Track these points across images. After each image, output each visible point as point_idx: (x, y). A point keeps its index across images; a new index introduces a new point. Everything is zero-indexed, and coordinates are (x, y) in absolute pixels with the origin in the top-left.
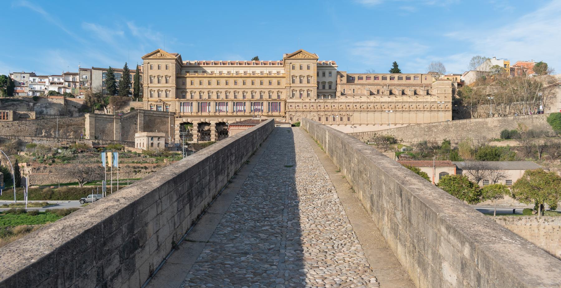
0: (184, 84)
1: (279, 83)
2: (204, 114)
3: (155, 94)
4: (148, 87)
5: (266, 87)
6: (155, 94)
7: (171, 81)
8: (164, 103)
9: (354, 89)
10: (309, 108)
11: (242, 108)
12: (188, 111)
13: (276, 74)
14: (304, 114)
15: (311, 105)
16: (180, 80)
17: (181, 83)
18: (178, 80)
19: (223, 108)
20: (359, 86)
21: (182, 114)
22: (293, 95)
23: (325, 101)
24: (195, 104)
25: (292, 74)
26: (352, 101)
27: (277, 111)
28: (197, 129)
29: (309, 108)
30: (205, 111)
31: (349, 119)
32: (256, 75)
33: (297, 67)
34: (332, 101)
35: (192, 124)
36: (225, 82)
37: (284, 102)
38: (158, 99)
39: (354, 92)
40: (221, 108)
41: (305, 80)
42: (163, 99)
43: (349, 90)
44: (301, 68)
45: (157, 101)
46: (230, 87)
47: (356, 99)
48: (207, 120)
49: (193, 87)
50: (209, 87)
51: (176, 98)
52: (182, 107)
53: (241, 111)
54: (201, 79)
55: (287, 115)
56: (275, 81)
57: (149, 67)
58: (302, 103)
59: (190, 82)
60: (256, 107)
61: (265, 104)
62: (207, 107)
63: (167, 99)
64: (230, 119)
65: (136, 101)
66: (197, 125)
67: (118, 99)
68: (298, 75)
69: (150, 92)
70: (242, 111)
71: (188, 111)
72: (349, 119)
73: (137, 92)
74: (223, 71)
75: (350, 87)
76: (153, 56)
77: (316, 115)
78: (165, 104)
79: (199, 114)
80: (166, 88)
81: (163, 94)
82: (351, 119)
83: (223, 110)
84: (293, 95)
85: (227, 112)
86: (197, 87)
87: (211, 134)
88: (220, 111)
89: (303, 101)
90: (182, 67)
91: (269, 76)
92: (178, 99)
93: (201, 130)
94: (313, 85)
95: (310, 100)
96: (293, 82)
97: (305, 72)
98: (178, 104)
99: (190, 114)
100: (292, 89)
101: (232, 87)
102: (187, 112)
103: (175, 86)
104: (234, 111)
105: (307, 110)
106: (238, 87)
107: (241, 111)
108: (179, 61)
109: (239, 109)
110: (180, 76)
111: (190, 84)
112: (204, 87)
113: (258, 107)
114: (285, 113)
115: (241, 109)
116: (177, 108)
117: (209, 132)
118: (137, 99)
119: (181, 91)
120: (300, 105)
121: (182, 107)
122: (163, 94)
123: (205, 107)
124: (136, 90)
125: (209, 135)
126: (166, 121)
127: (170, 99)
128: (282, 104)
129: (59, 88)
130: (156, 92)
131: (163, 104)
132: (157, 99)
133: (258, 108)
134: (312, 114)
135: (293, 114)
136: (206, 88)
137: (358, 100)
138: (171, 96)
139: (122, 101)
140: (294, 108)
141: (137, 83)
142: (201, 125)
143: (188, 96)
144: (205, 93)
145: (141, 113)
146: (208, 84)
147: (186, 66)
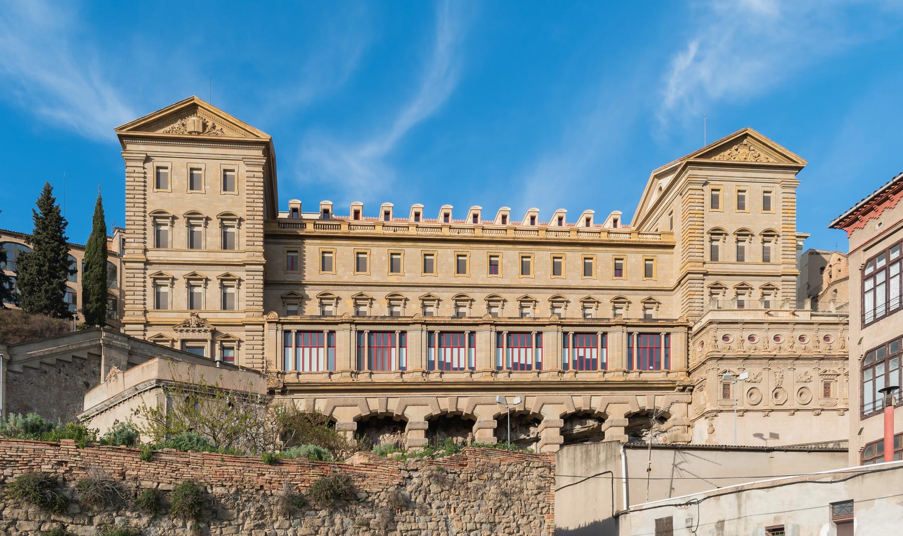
0: (295, 263)
2: (380, 377)
3: (178, 296)
4: (147, 263)
6: (178, 296)
7: (243, 240)
8: (214, 333)
10: (792, 347)
11: (527, 356)
12: (314, 369)
14: (774, 369)
15: (797, 334)
16: (280, 249)
17: (282, 260)
18: (273, 247)
19: (457, 356)
21: (290, 378)
24: (345, 338)
25: (709, 226)
27: (658, 367)
29: (792, 347)
30: (385, 367)
33: (728, 195)
36: (453, 260)
40: (448, 354)
41: (753, 248)
42: (212, 318)
48: (394, 405)
49: (328, 277)
50: (393, 279)
51: (264, 313)
52: (291, 351)
53: (526, 367)
54: (361, 245)
58: (766, 326)
59: (318, 258)
60: (581, 351)
61: (617, 339)
63: (225, 316)
64: (483, 401)
67: (10, 320)
69: (156, 286)
70: (529, 367)
71: (314, 369)
73: (95, 305)
77: (815, 375)
78: (218, 338)
79: (363, 378)
81: (211, 295)
83: (455, 365)
85: (472, 370)
86: (346, 279)
88: (445, 367)
89: (770, 319)
92: (274, 315)
94: (780, 269)
95: (794, 314)
96: (714, 257)
97: (758, 222)
98: (273, 335)
99: (323, 378)
100: (710, 281)
101: (480, 282)
102: (310, 373)
103: (263, 260)
104: (499, 369)
105: (784, 353)
107: (526, 367)
109: (516, 360)
111: (318, 264)
112: (375, 278)
113: (588, 350)
115: (523, 362)
116: (271, 353)
120: (759, 334)
121: (291, 351)
122: (211, 295)
123: (386, 353)
124: (92, 298)
128: (677, 339)
130: (181, 285)
131: (208, 336)
133: (588, 356)
134: (802, 368)
138: (243, 305)
139: (26, 327)
141: (97, 270)
143: (312, 308)
144: (375, 304)
146: (387, 267)
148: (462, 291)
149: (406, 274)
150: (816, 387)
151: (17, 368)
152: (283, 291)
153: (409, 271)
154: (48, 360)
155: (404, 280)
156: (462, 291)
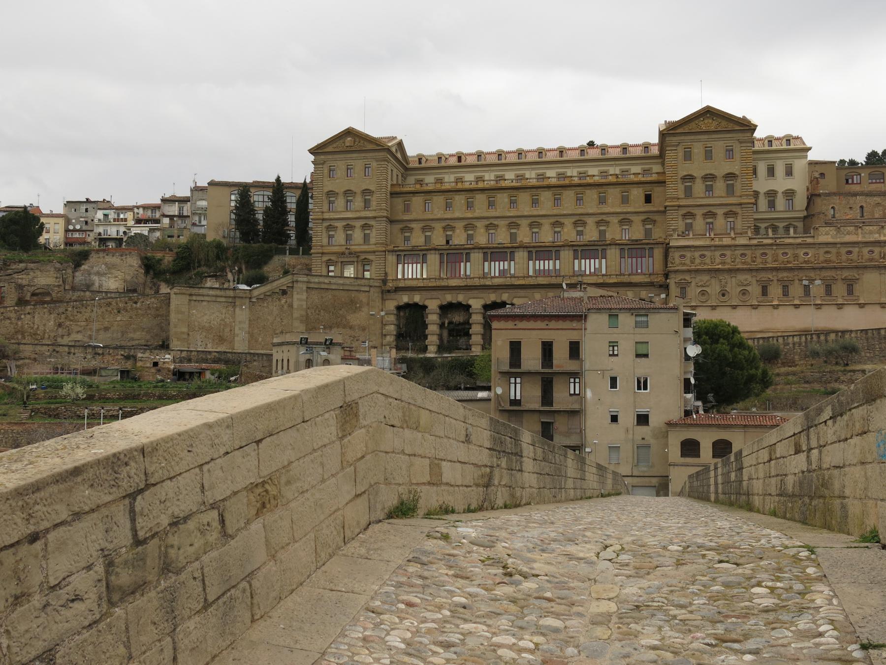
1: (648, 199)
5: (612, 210)
6: (340, 237)
9: (862, 207)
13: (640, 176)
20: (877, 199)
22: (689, 227)
23: (778, 241)
26: (860, 239)
28: (438, 321)
31: (850, 292)
32: (589, 180)
34: (799, 241)
35: (470, 306)
37: (660, 246)
38: (344, 248)
39: (862, 216)
43: (847, 211)
44: (708, 155)
45: (343, 253)
46: (519, 214)
47: (871, 233)
55: (672, 282)
56: (637, 194)
57: (326, 171)
62: (462, 264)
63: (365, 248)
65: (298, 254)
66: (438, 311)
68: (698, 173)
72: (850, 292)
74: (504, 175)
75: (851, 202)
76: (335, 145)
80: (362, 222)
81: (358, 235)
82: (857, 288)
84: (689, 227)
86: (439, 216)
87: (471, 331)
90: (406, 169)
91: (621, 180)
93: (447, 322)
101: (526, 214)
106: (541, 213)
108: (399, 156)
110: (398, 189)
112: (457, 214)
114: (666, 276)
117: (467, 326)
118: (301, 248)
119: (401, 226)
122: (358, 235)
125: (468, 335)
126: (361, 301)
127: (372, 248)
129: (151, 230)
132: (343, 249)
135: (687, 277)
136: (461, 216)
137: (876, 237)
140: (688, 262)
142: (446, 309)
145: (301, 282)
147: (417, 165)
148: (514, 220)
149: (477, 211)
150: (755, 290)
151: (254, 300)
152: (401, 226)
153: (478, 209)
154: (268, 294)
155: (476, 215)
156: (514, 220)
